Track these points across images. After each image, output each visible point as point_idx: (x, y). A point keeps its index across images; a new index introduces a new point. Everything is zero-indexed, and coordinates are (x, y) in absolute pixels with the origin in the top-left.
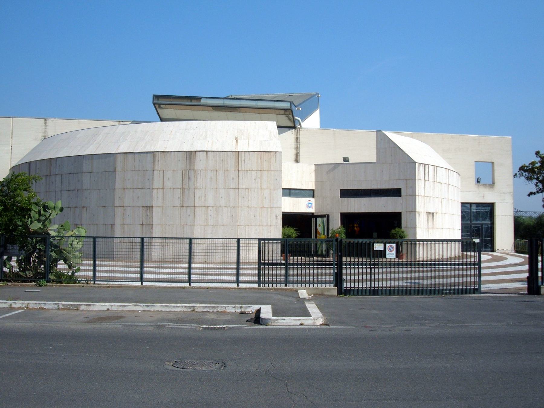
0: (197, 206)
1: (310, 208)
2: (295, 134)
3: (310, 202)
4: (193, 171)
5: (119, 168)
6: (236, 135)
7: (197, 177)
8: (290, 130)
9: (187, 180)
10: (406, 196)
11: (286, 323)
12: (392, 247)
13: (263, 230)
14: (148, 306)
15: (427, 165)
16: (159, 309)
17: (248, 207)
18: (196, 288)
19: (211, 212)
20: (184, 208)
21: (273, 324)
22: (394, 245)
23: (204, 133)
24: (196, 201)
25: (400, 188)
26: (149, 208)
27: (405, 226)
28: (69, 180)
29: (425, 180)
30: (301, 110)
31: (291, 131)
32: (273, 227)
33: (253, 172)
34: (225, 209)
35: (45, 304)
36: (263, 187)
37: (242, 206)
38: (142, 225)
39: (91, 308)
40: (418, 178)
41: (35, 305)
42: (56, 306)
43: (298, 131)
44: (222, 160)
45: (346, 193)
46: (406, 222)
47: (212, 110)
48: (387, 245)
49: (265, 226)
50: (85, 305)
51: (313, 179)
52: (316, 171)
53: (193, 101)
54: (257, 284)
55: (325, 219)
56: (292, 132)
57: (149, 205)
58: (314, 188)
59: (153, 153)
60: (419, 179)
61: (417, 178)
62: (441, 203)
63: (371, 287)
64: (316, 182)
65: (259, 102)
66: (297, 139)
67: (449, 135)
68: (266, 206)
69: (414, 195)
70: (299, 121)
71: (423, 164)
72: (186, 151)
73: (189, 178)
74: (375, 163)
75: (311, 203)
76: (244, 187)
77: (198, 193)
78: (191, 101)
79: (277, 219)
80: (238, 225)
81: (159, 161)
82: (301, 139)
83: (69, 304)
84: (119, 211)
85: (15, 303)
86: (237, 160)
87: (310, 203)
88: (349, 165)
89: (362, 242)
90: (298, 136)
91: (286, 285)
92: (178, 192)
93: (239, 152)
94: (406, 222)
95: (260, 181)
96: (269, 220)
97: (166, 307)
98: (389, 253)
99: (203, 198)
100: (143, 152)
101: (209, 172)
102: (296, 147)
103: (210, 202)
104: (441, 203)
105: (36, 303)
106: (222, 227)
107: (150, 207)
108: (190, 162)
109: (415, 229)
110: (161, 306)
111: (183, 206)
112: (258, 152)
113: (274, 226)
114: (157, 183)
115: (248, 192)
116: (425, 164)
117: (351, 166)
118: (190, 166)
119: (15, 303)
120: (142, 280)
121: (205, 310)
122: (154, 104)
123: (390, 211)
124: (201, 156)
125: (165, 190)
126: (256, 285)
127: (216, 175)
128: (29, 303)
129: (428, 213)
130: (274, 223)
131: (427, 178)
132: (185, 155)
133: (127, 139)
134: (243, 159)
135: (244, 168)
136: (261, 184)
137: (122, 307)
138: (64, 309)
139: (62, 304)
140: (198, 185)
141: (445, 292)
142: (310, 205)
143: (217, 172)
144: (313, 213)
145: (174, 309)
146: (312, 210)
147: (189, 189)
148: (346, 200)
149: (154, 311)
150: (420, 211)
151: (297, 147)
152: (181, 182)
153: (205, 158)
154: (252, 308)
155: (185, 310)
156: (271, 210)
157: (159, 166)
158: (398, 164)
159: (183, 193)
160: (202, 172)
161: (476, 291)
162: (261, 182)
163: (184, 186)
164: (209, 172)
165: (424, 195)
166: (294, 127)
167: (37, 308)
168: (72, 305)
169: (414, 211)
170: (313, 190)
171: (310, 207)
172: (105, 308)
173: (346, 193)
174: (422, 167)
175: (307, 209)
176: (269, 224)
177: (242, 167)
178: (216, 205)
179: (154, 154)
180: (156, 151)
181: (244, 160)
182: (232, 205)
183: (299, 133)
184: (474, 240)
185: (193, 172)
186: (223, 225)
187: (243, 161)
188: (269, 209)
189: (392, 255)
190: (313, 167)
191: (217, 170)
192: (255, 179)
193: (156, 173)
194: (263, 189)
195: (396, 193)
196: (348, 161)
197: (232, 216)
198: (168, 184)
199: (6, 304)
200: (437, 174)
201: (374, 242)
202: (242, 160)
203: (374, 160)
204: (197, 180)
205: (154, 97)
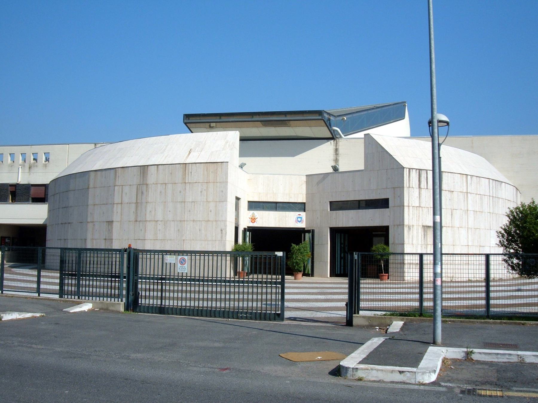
0: (148, 220)
1: (300, 223)
2: (334, 145)
3: (300, 216)
4: (145, 185)
5: (91, 186)
7: (148, 191)
8: (328, 141)
10: (394, 207)
13: (208, 244)
15: (425, 171)
17: (194, 221)
19: (160, 227)
20: (138, 222)
24: (148, 215)
26: (110, 223)
29: (420, 187)
30: (346, 119)
31: (329, 142)
32: (217, 242)
33: (200, 184)
34: (172, 223)
37: (188, 220)
38: (105, 239)
40: (408, 186)
43: (338, 142)
44: (171, 173)
45: (336, 206)
46: (394, 238)
49: (210, 240)
51: (304, 192)
52: (307, 182)
53: (222, 118)
54: (58, 295)
55: (311, 234)
56: (331, 143)
57: (110, 220)
58: (304, 201)
60: (409, 187)
61: (405, 186)
62: (452, 214)
64: (307, 194)
66: (336, 150)
68: (211, 219)
70: (337, 131)
71: (417, 169)
73: (142, 193)
74: (362, 170)
75: (301, 218)
76: (190, 200)
77: (149, 207)
79: (222, 233)
80: (184, 240)
82: (341, 151)
84: (90, 226)
87: (299, 218)
90: (338, 147)
91: (79, 298)
92: (133, 206)
93: (186, 164)
95: (205, 194)
96: (214, 235)
98: (181, 267)
99: (153, 212)
101: (159, 185)
102: (335, 159)
103: (159, 217)
104: (452, 214)
106: (169, 241)
107: (111, 221)
109: (403, 245)
111: (136, 221)
114: (117, 200)
115: (194, 205)
116: (420, 170)
117: (340, 175)
118: (143, 180)
122: (186, 123)
123: (378, 225)
124: (153, 170)
125: (123, 205)
126: (57, 297)
131: (422, 186)
134: (190, 170)
135: (191, 180)
136: (207, 196)
140: (149, 200)
141: (241, 315)
142: (299, 219)
143: (166, 186)
144: (304, 228)
146: (302, 225)
147: (142, 203)
150: (411, 224)
151: (337, 159)
152: (135, 196)
157: (119, 182)
158: (386, 170)
159: (137, 207)
161: (279, 317)
162: (207, 194)
163: (138, 201)
164: (159, 185)
165: (418, 205)
166: (332, 138)
169: (402, 225)
170: (304, 203)
171: (299, 222)
173: (336, 206)
174: (414, 175)
175: (296, 224)
177: (189, 180)
178: (164, 219)
179: (115, 170)
183: (338, 145)
184: (276, 253)
185: (145, 187)
186: (171, 240)
187: (190, 174)
188: (214, 223)
189: (184, 269)
190: (304, 178)
191: (166, 184)
192: (201, 192)
193: (116, 188)
194: (209, 202)
195: (383, 203)
197: (179, 230)
198: (126, 200)
202: (189, 173)
203: (362, 168)
205: (185, 117)
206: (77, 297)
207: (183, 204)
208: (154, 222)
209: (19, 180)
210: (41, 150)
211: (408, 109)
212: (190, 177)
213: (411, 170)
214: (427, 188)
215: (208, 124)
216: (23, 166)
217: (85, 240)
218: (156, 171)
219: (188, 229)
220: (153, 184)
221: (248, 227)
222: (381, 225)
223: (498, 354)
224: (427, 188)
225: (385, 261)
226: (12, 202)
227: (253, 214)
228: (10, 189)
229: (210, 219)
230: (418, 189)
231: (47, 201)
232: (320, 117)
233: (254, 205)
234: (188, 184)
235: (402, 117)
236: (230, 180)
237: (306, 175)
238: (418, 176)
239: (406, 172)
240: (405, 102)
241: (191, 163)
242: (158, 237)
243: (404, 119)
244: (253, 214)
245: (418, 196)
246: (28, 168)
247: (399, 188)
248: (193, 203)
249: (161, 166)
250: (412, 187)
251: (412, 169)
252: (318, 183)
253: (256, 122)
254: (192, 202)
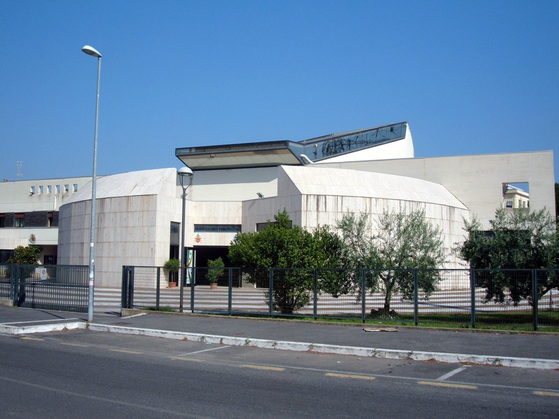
5: (73, 215)
17: (133, 242)
26: (82, 244)
33: (138, 213)
38: (80, 257)
40: (305, 209)
51: (240, 215)
52: (243, 207)
53: (206, 150)
58: (241, 224)
60: (307, 211)
61: (302, 210)
63: (33, 302)
67: (470, 157)
68: (145, 241)
70: (304, 158)
71: (315, 195)
73: (101, 220)
77: (105, 231)
78: (257, 147)
84: (72, 246)
103: (112, 239)
116: (318, 196)
122: (177, 156)
124: (108, 201)
131: (320, 209)
134: (131, 202)
140: (106, 225)
159: (98, 231)
170: (240, 225)
186: (118, 257)
187: (131, 204)
190: (240, 204)
191: (116, 213)
200: (342, 204)
203: (276, 195)
208: (108, 243)
209: (55, 208)
210: (70, 182)
211: (410, 128)
213: (309, 196)
214: (326, 211)
215: (209, 156)
216: (58, 196)
217: (69, 257)
220: (108, 212)
221: (194, 246)
223: (99, 326)
224: (326, 211)
225: (130, 272)
226: (51, 226)
227: (198, 234)
228: (48, 215)
230: (316, 212)
231: (57, 226)
232: (285, 147)
233: (199, 228)
235: (401, 136)
236: (159, 208)
237: (242, 201)
238: (316, 201)
239: (304, 198)
240: (406, 123)
243: (404, 138)
244: (198, 235)
245: (316, 219)
246: (61, 197)
250: (310, 211)
251: (310, 195)
252: (250, 207)
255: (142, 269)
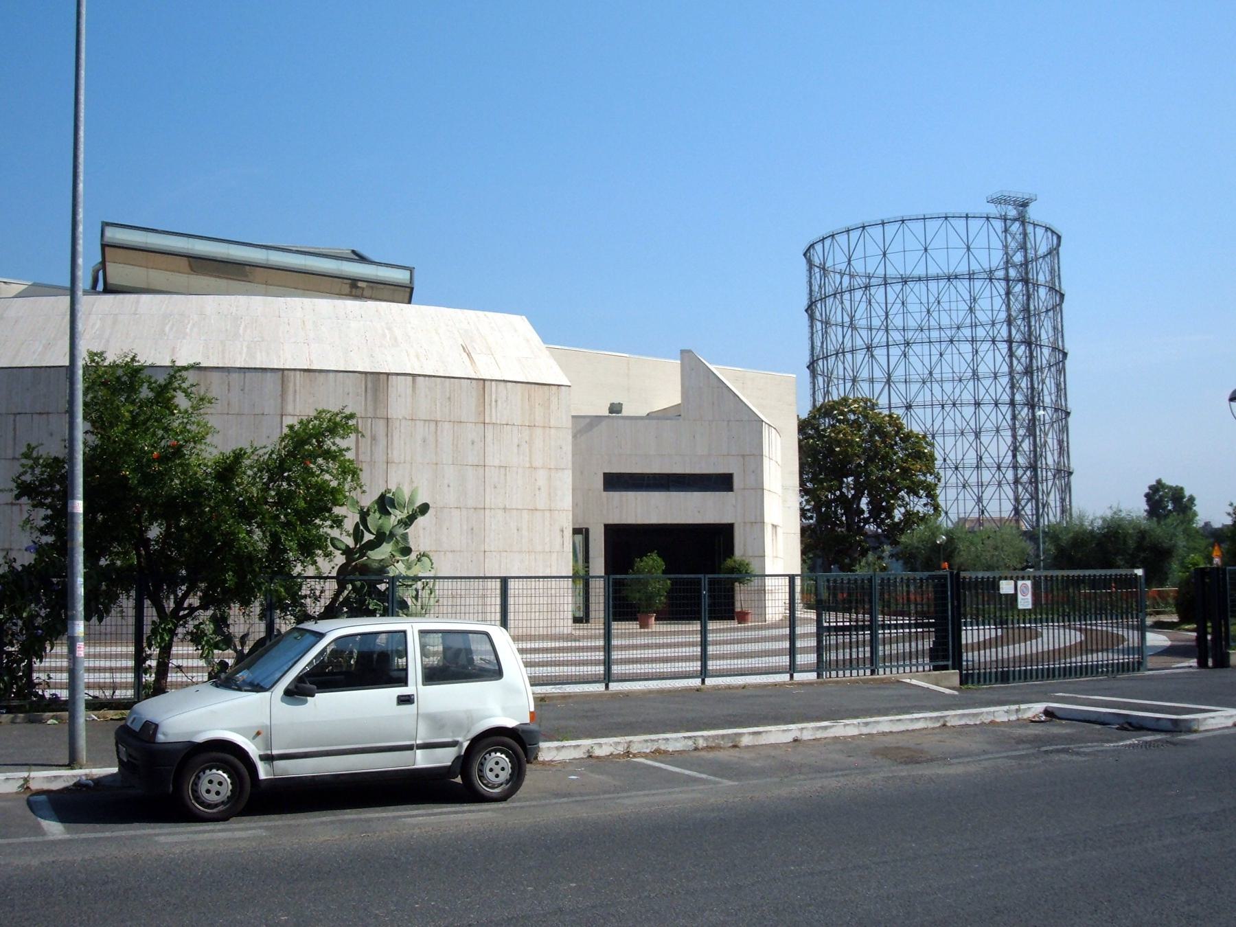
6: (460, 342)
7: (392, 436)
9: (369, 442)
10: (744, 489)
11: (1216, 724)
12: (1026, 586)
14: (866, 724)
16: (886, 728)
18: (719, 689)
21: (1202, 728)
22: (1029, 583)
23: (386, 331)
25: (731, 472)
27: (742, 553)
28: (15, 429)
32: (554, 556)
33: (515, 428)
34: (456, 513)
35: (667, 739)
36: (534, 466)
39: (763, 740)
41: (645, 745)
42: (690, 743)
44: (449, 398)
45: (614, 482)
46: (745, 545)
47: (187, 269)
48: (1020, 583)
49: (540, 552)
50: (749, 733)
59: (281, 372)
65: (345, 263)
69: (759, 489)
72: (366, 373)
73: (374, 438)
76: (497, 463)
81: (298, 391)
83: (717, 736)
85: (600, 745)
86: (482, 400)
88: (621, 422)
89: (983, 578)
91: (873, 672)
93: (484, 380)
94: (745, 545)
95: (527, 450)
96: (547, 540)
97: (898, 723)
100: (251, 368)
105: (646, 741)
106: (450, 555)
108: (376, 400)
109: (762, 559)
110: (891, 721)
112: (524, 385)
113: (558, 552)
115: (505, 475)
118: (375, 409)
119: (600, 745)
120: (608, 678)
121: (963, 722)
123: (712, 521)
124: (399, 388)
127: (436, 433)
128: (630, 742)
129: (773, 525)
130: (557, 547)
132: (363, 382)
133: (188, 330)
134: (494, 397)
135: (497, 419)
137: (821, 731)
138: (709, 748)
139: (702, 736)
140: (395, 455)
145: (911, 727)
147: (372, 463)
148: (616, 495)
149: (879, 734)
153: (409, 391)
154: (1033, 710)
155: (930, 725)
156: (551, 517)
158: (726, 423)
160: (403, 422)
162: (530, 451)
167: (648, 751)
168: (723, 736)
169: (759, 522)
172: (788, 738)
173: (614, 482)
176: (547, 550)
177: (491, 417)
180: (288, 367)
181: (496, 401)
182: (471, 503)
185: (382, 423)
187: (493, 403)
188: (547, 514)
191: (436, 422)
195: (722, 482)
196: (620, 412)
197: (472, 529)
199: (578, 750)
201: (1000, 578)
202: (491, 401)
204: (392, 443)
206: (868, 672)
207: (481, 470)
212: (494, 410)
218: (411, 389)
219: (493, 527)
222: (717, 521)
229: (538, 507)
234: (491, 426)
241: (496, 380)
242: (421, 546)
247: (755, 457)
248: (502, 470)
249: (422, 378)
253: (295, 274)
254: (500, 467)
255: (533, 583)
